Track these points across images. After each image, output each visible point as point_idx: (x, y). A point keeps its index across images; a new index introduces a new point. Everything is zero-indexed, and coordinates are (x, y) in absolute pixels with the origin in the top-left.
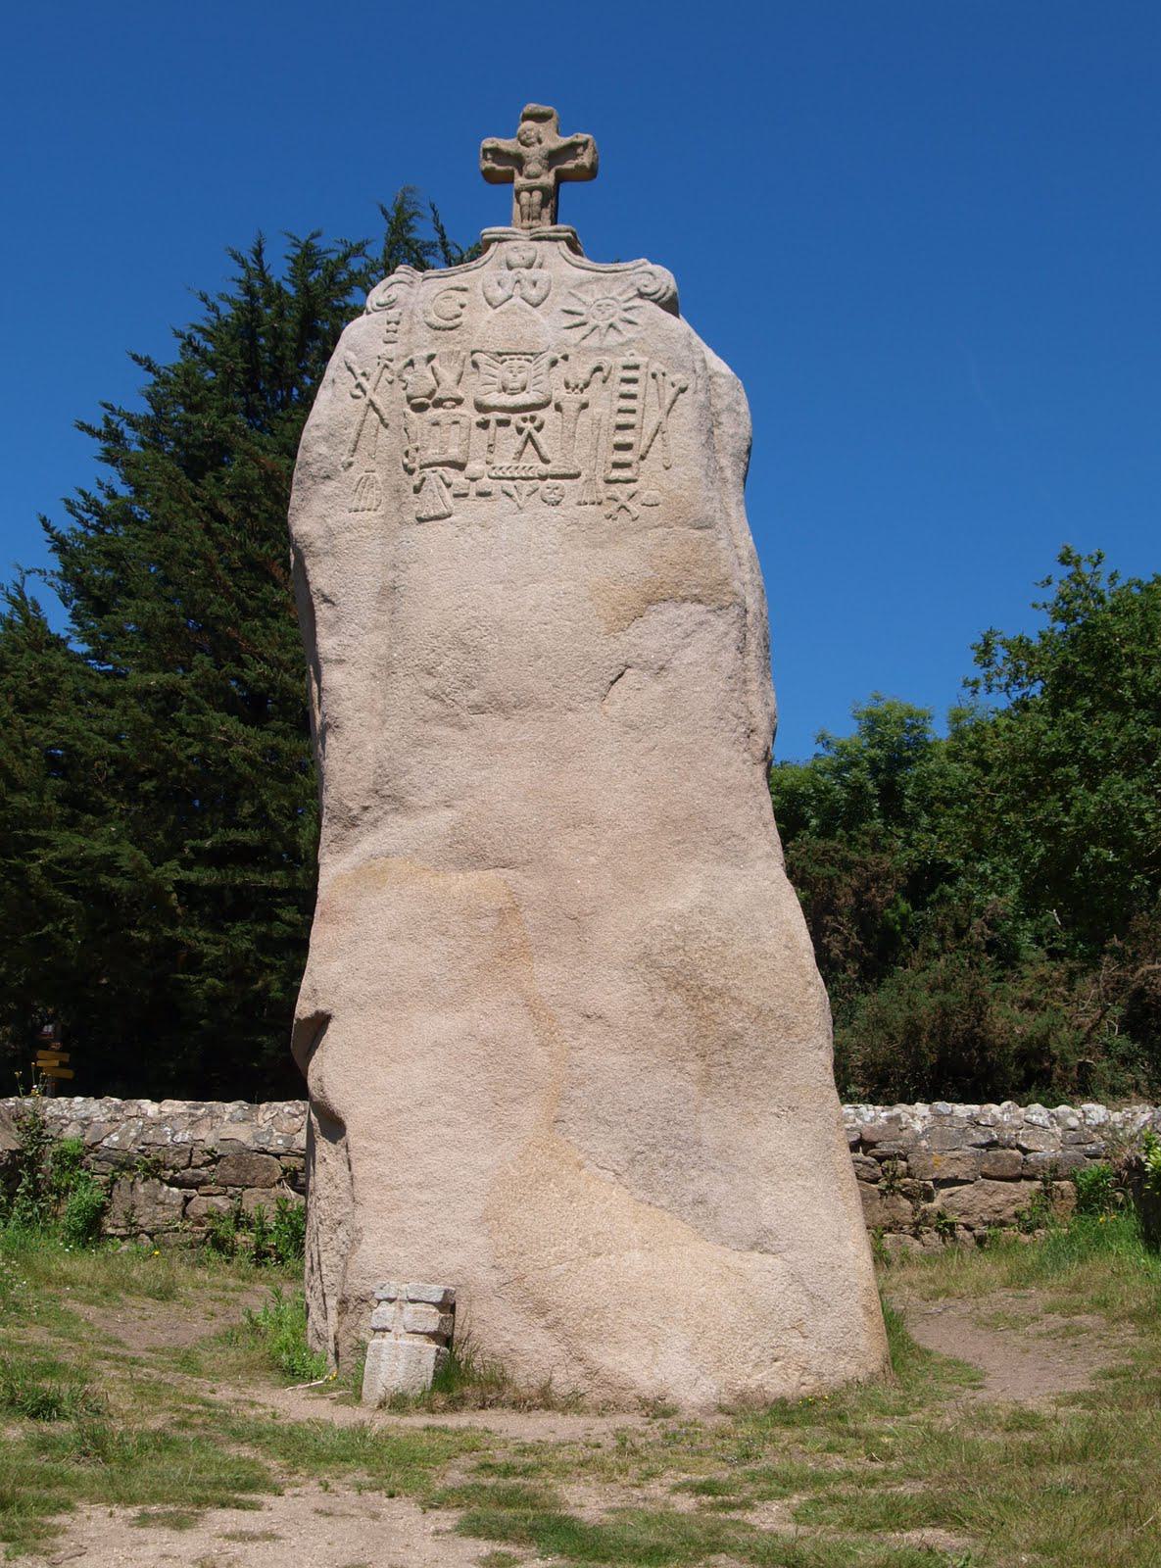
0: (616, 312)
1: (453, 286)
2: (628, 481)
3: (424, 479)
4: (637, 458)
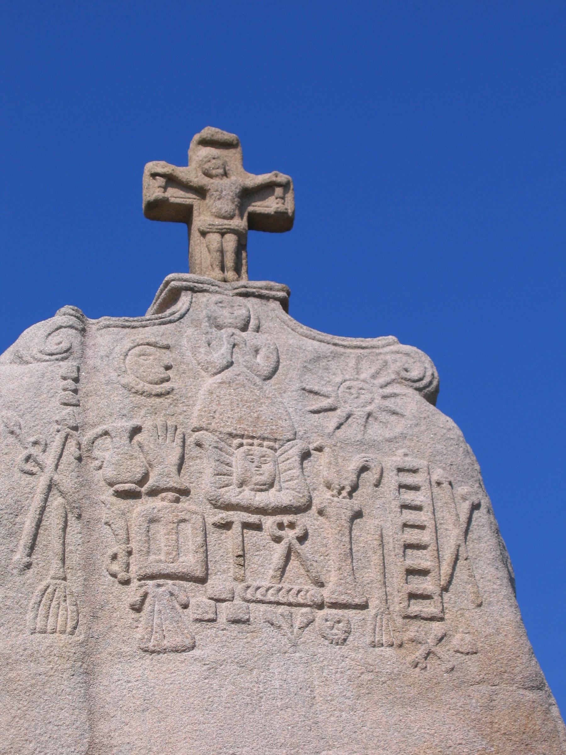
0: (373, 400)
2: (432, 619)
4: (438, 590)
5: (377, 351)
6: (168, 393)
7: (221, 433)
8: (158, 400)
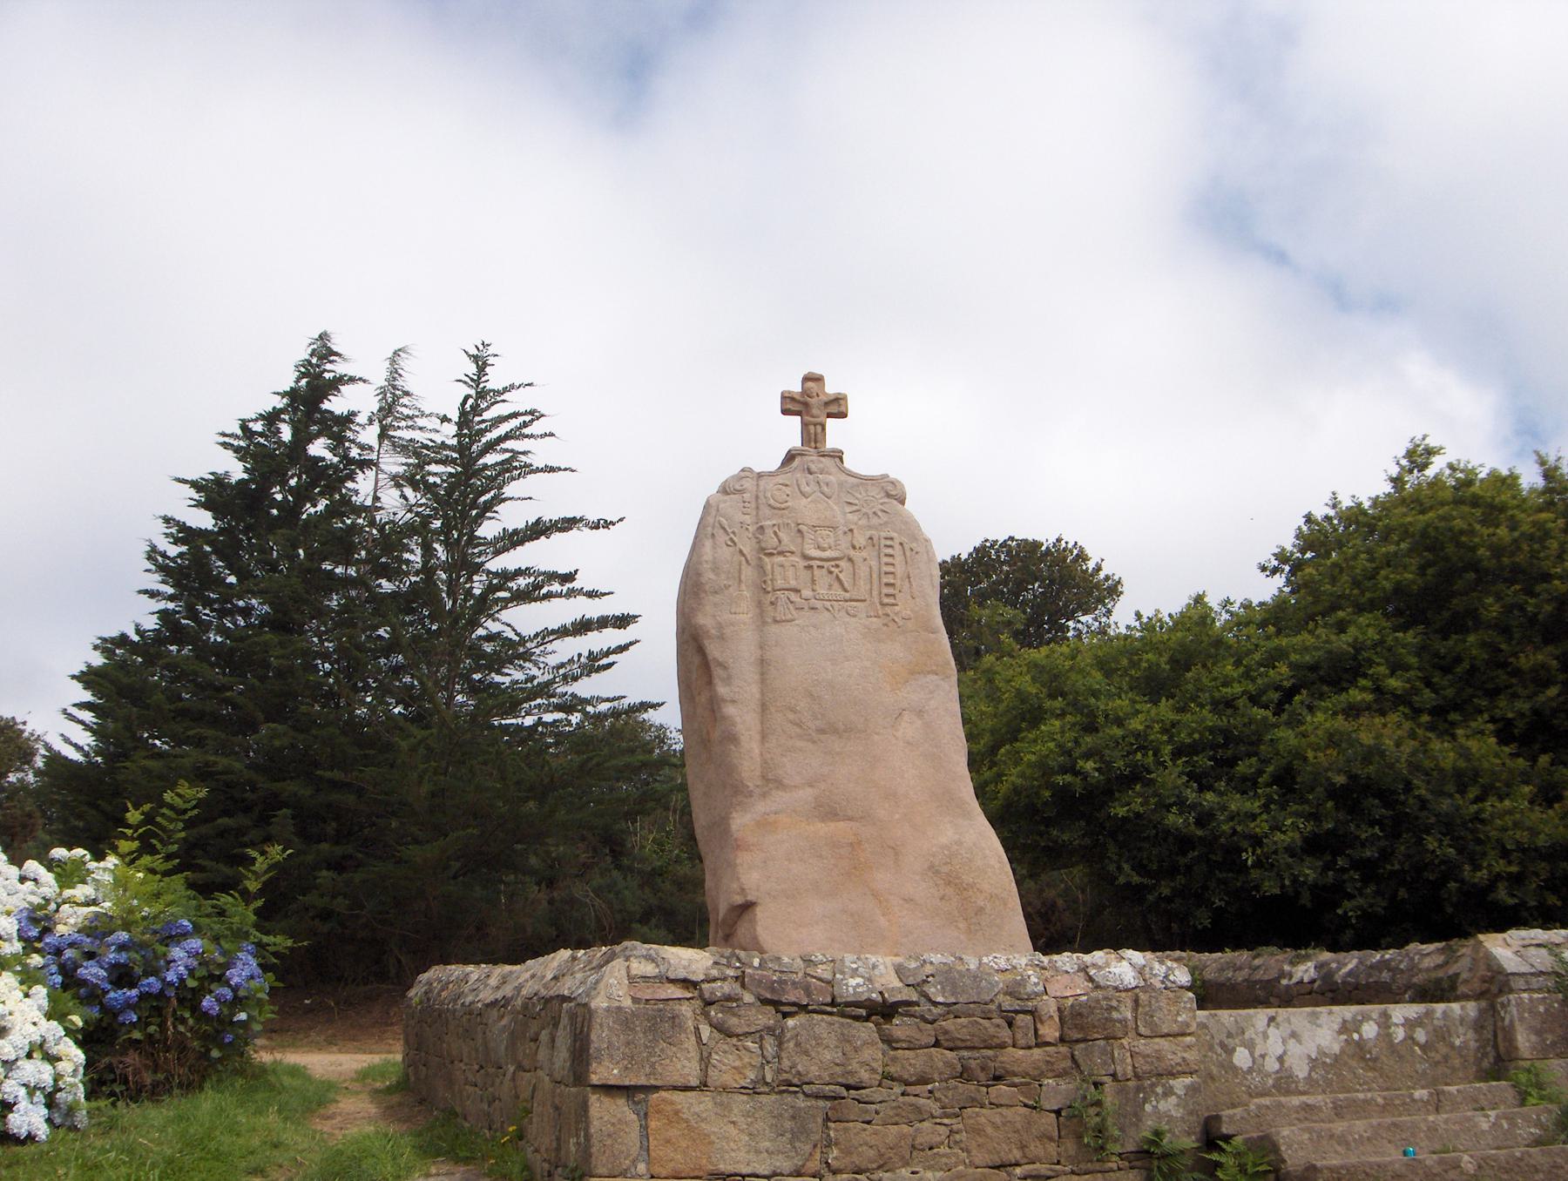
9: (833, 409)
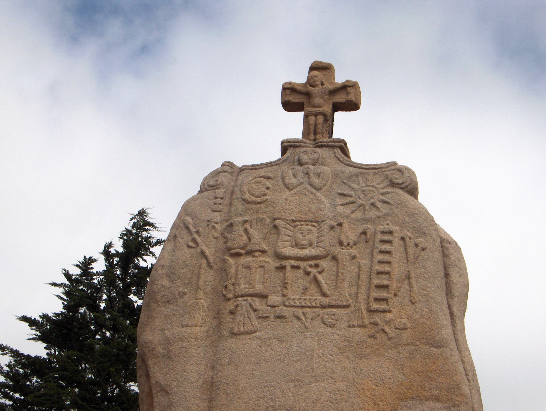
1: (261, 175)
3: (237, 306)
5: (384, 170)
6: (265, 201)
7: (287, 220)
8: (259, 206)
9: (340, 98)
